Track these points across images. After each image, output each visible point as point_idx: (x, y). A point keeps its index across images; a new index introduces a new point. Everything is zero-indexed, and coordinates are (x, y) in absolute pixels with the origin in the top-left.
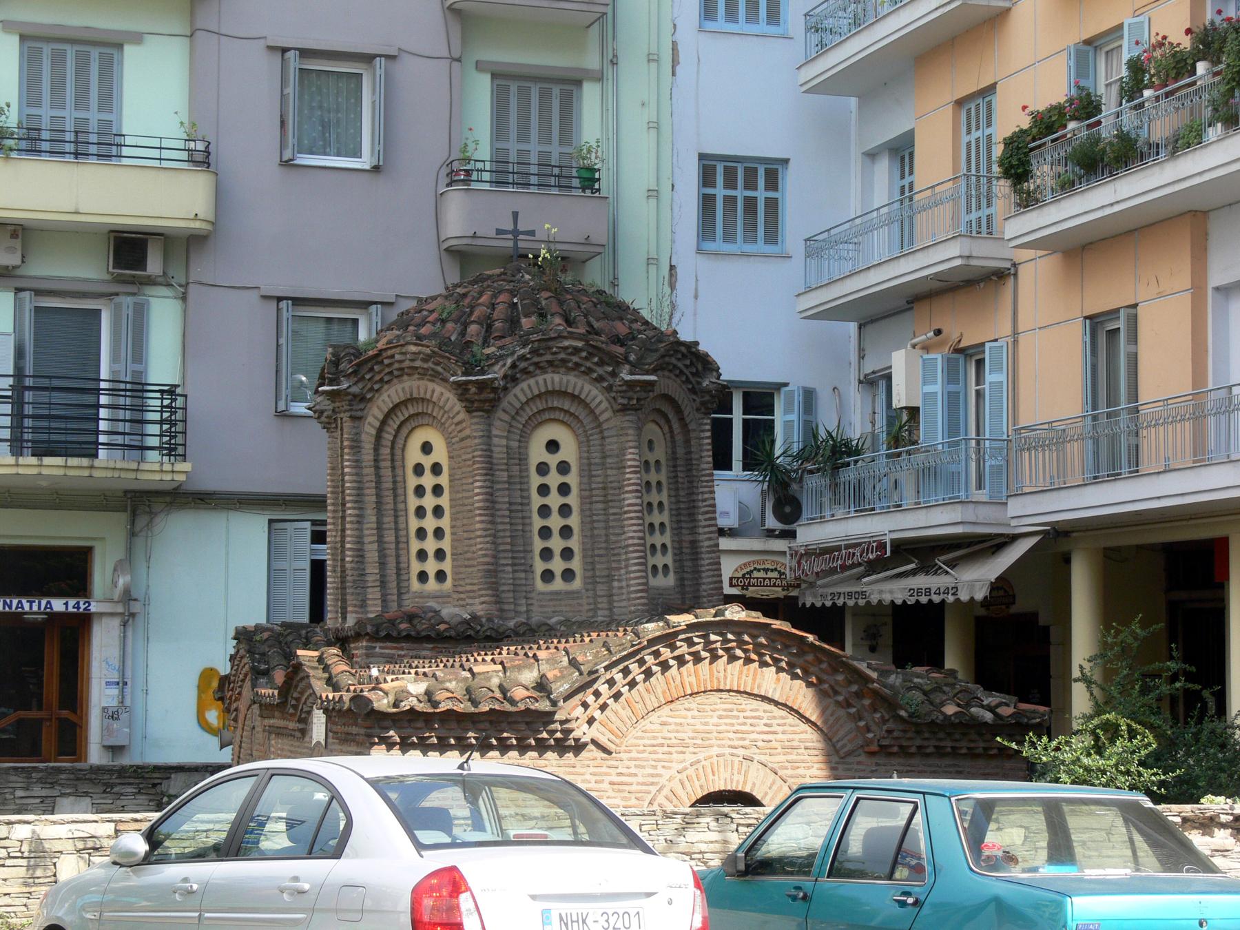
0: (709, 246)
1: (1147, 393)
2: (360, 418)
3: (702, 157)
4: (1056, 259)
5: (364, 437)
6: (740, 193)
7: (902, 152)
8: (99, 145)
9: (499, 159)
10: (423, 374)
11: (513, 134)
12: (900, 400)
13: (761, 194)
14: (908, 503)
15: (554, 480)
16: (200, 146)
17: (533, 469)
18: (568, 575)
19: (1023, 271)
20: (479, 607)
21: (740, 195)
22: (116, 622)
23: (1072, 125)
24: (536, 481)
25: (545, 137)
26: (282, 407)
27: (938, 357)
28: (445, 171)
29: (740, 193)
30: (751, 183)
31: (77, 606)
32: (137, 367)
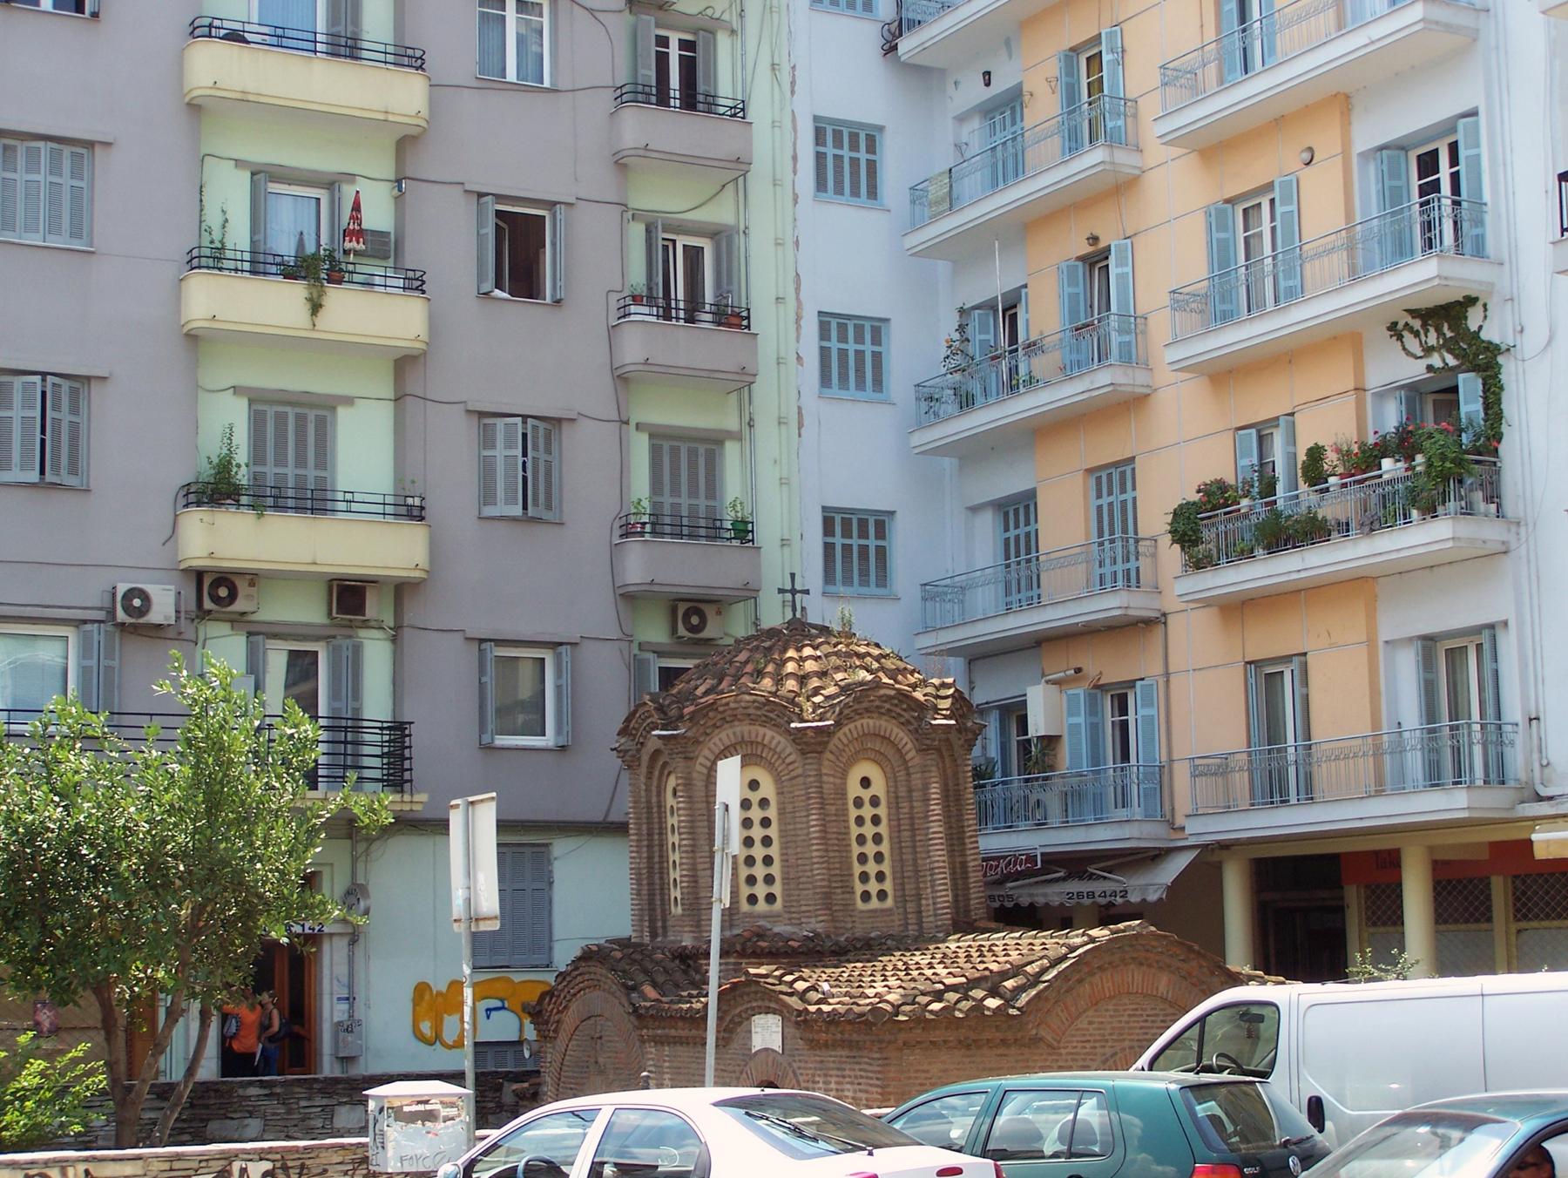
0: (831, 589)
1: (1321, 732)
3: (824, 509)
4: (1214, 611)
5: (695, 775)
6: (855, 542)
7: (1018, 511)
8: (315, 501)
9: (656, 515)
10: (753, 720)
11: (667, 489)
12: (1038, 725)
13: (872, 542)
14: (1055, 818)
15: (867, 812)
16: (417, 502)
17: (851, 803)
18: (882, 895)
19: (1170, 619)
20: (815, 924)
21: (856, 544)
22: (345, 942)
23: (1245, 502)
24: (853, 813)
25: (693, 493)
26: (486, 739)
27: (1080, 691)
28: (617, 524)
29: (855, 542)
30: (863, 534)
32: (356, 705)
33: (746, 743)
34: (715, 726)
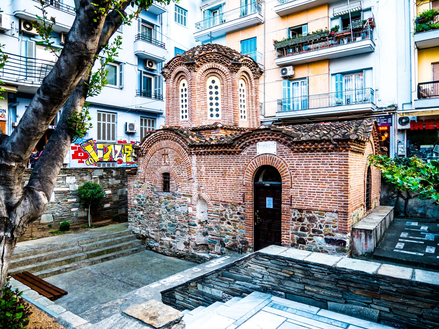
34: (204, 62)
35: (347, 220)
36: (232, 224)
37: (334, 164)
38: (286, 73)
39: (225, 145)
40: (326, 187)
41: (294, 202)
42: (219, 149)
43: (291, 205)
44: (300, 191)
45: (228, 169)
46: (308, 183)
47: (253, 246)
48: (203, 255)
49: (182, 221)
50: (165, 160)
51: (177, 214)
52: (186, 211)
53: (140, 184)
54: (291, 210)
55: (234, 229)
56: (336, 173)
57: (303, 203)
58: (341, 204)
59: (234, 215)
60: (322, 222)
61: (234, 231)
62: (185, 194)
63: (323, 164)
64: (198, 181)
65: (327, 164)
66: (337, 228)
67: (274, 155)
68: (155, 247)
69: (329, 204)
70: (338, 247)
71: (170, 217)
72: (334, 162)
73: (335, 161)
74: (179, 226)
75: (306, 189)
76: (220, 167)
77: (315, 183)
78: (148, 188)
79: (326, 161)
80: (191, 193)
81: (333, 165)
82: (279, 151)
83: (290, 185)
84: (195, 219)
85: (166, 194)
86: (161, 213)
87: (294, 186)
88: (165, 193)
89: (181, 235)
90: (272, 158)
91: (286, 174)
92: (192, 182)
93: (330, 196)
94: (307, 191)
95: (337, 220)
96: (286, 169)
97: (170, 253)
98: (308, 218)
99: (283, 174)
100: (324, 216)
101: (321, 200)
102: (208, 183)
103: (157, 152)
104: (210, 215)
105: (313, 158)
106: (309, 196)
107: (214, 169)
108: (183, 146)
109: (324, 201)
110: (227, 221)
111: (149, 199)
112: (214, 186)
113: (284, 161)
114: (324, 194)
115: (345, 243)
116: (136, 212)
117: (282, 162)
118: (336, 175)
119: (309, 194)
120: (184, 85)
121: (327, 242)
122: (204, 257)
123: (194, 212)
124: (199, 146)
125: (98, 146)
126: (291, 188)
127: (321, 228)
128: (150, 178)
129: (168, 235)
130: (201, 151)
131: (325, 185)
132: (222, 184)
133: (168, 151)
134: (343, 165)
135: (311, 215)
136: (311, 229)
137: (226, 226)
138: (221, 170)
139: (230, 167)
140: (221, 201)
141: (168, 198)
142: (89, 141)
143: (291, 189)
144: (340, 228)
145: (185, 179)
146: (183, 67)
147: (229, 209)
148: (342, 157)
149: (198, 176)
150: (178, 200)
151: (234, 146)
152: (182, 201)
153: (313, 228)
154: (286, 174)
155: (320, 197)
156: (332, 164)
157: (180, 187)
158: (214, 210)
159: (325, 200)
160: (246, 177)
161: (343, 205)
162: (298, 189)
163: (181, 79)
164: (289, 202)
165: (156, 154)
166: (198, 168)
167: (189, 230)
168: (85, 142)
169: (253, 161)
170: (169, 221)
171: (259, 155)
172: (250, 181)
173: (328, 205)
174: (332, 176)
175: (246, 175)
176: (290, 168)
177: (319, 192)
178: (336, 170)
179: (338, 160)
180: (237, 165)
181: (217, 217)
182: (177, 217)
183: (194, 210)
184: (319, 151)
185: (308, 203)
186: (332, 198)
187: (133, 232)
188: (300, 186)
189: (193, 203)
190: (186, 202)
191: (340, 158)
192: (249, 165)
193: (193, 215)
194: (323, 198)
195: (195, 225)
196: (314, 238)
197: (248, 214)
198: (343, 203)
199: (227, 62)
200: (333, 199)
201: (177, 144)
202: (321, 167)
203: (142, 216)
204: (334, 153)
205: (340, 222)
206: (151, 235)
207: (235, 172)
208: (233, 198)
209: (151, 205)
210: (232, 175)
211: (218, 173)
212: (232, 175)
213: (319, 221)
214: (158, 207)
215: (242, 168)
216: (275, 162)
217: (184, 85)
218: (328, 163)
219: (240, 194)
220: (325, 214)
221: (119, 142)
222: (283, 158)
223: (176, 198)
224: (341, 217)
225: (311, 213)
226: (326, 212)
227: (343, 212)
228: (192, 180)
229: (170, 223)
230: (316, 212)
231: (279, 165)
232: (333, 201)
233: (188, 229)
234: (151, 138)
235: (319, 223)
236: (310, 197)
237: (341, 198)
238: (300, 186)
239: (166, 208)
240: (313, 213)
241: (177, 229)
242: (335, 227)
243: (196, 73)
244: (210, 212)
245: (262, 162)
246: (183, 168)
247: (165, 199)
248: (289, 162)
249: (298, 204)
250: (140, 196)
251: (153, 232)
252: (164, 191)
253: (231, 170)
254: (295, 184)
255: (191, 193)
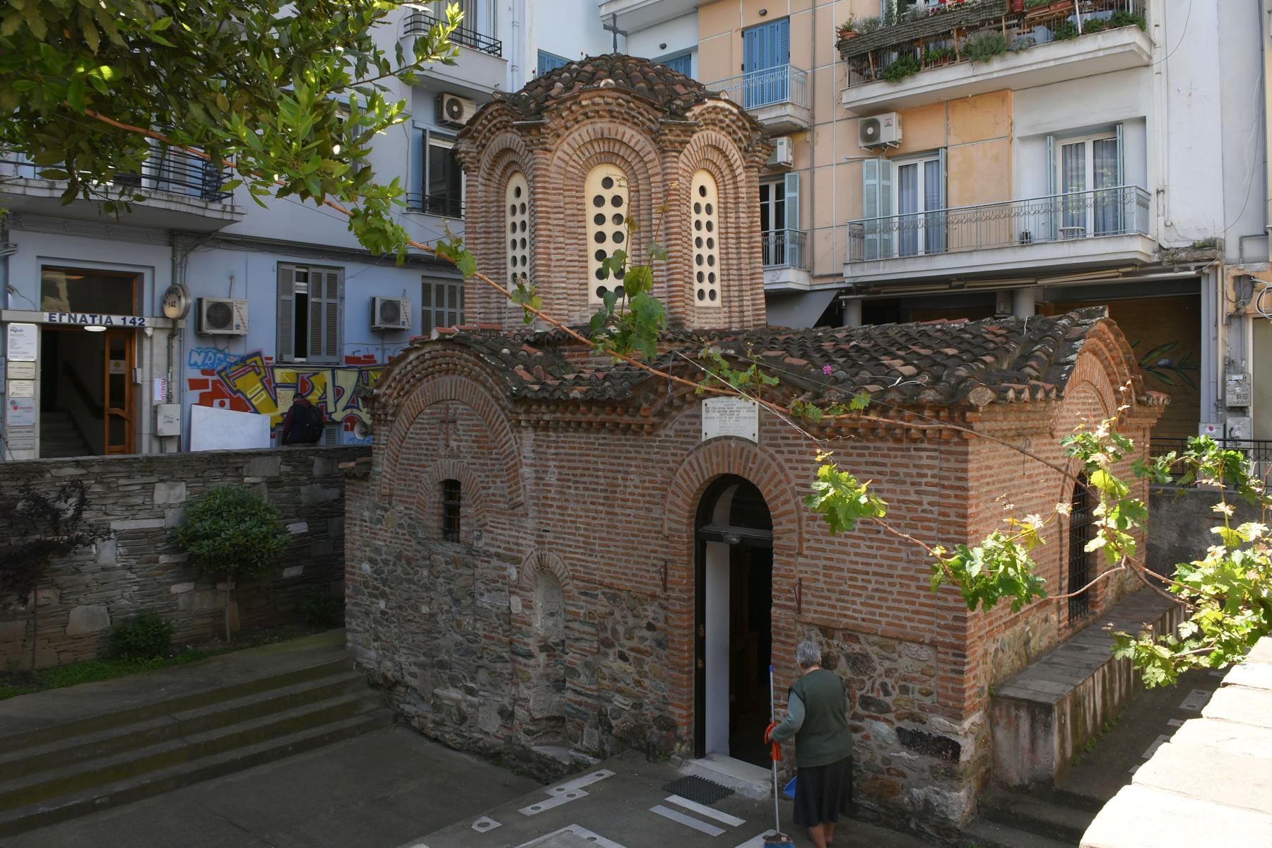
2: (550, 151)
31: (133, 321)
33: (603, 139)
35: (962, 672)
36: (631, 659)
37: (926, 484)
38: (876, 136)
39: (611, 405)
40: (900, 559)
41: (807, 603)
42: (596, 415)
43: (799, 610)
44: (825, 567)
45: (620, 482)
46: (850, 541)
47: (692, 736)
48: (550, 752)
49: (492, 638)
50: (447, 440)
51: (479, 613)
52: (504, 610)
53: (378, 512)
54: (799, 628)
55: (637, 677)
56: (932, 512)
57: (834, 607)
58: (944, 618)
59: (638, 633)
60: (889, 672)
61: (638, 683)
62: (501, 551)
63: (892, 482)
64: (536, 514)
65: (904, 482)
66: (934, 697)
67: (751, 442)
68: (419, 716)
69: (909, 615)
70: (936, 761)
71: (459, 624)
72: (925, 476)
73: (929, 472)
74: (485, 656)
75: (844, 561)
76: (600, 473)
77: (868, 543)
78: (401, 526)
79: (902, 471)
80: (519, 551)
81: (924, 488)
82: (766, 431)
83: (796, 544)
84: (530, 636)
85: (450, 549)
86: (436, 610)
87: (809, 548)
88: (448, 544)
89: (491, 684)
90: (745, 453)
91: (787, 507)
92: (522, 516)
93: (913, 590)
94: (846, 566)
95: (933, 672)
96: (784, 491)
97: (459, 740)
98: (848, 657)
99: (776, 508)
100: (895, 656)
101: (886, 600)
102: (565, 521)
103: (427, 411)
104: (570, 624)
105: (862, 460)
106: (850, 586)
107: (584, 479)
108: (497, 399)
109: (896, 605)
110: (618, 648)
111: (404, 561)
112: (582, 532)
113: (780, 466)
114: (895, 580)
115: (956, 749)
116: (366, 600)
117: (774, 465)
118: (929, 520)
119: (851, 579)
120: (518, 192)
121: (903, 743)
122: (553, 760)
123: (527, 612)
124: (539, 402)
125: (280, 375)
126: (800, 554)
127: (887, 693)
128: (406, 493)
129: (454, 682)
130: (546, 417)
131: (898, 551)
132: (605, 529)
133: (456, 409)
134: (952, 487)
135: (857, 648)
136: (859, 693)
137: (614, 666)
138: (602, 481)
139: (627, 473)
140: (602, 584)
141: (454, 562)
142: (248, 361)
143: (801, 559)
144: (941, 700)
145: (501, 505)
146: (514, 136)
147: (622, 609)
148: (948, 460)
149: (538, 498)
150: (482, 568)
151: (638, 409)
152: (493, 574)
153: (863, 692)
154: (787, 507)
155: (884, 591)
156: (920, 484)
157: (488, 528)
158: (582, 612)
159: (900, 601)
160: (671, 511)
161: (950, 622)
162: (818, 558)
163: (509, 172)
164: (792, 600)
165: (424, 418)
166: (536, 472)
167: (514, 669)
168: (236, 364)
169: (692, 458)
170: (459, 638)
171: (709, 442)
172: (683, 524)
173: (906, 618)
174: (920, 524)
175: (672, 503)
176: (797, 488)
177: (882, 575)
178: (931, 504)
179: (935, 472)
180: (646, 467)
181: (589, 634)
182: (478, 625)
183: (528, 605)
184: (882, 439)
185: (848, 609)
186: (918, 596)
187: (359, 664)
188: (824, 550)
189: (525, 582)
190: (504, 577)
191: (945, 465)
192: (681, 470)
193: (525, 623)
194: (891, 593)
195: (529, 655)
196: (866, 724)
197: (677, 632)
198: (950, 615)
199: (650, 120)
200: (922, 600)
201: (482, 389)
202: (888, 491)
203: (383, 613)
204: (926, 445)
205: (942, 678)
206: (408, 679)
207: (640, 491)
208: (634, 575)
209: (410, 581)
210: (634, 501)
211: (594, 490)
212: (634, 501)
213: (880, 670)
214: (428, 589)
215: (659, 478)
216: (755, 467)
217: (518, 192)
218: (909, 480)
219: (654, 565)
220: (899, 648)
221: (348, 359)
222: (777, 456)
223: (478, 563)
224: (944, 661)
225: (857, 640)
226: (901, 640)
227: (952, 646)
228: (520, 510)
229: (461, 644)
230: (871, 639)
231: (767, 477)
232: (922, 604)
233: (509, 665)
234: (409, 367)
235: (880, 676)
236: (854, 587)
237: (946, 600)
238: (824, 550)
239: (450, 592)
240: (862, 640)
241: (480, 662)
242: (928, 694)
243: (549, 156)
244: (570, 617)
245: (718, 464)
246: (497, 467)
247: (447, 563)
248: (796, 469)
249: (820, 608)
250: (377, 550)
251: (414, 669)
252: (447, 539)
253: (629, 483)
254: (812, 544)
255: (519, 551)
